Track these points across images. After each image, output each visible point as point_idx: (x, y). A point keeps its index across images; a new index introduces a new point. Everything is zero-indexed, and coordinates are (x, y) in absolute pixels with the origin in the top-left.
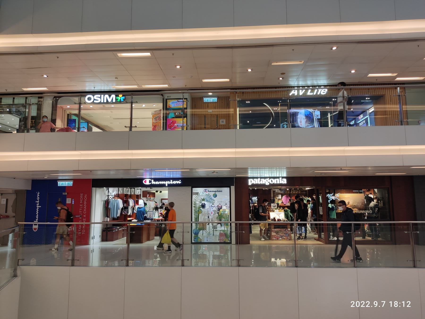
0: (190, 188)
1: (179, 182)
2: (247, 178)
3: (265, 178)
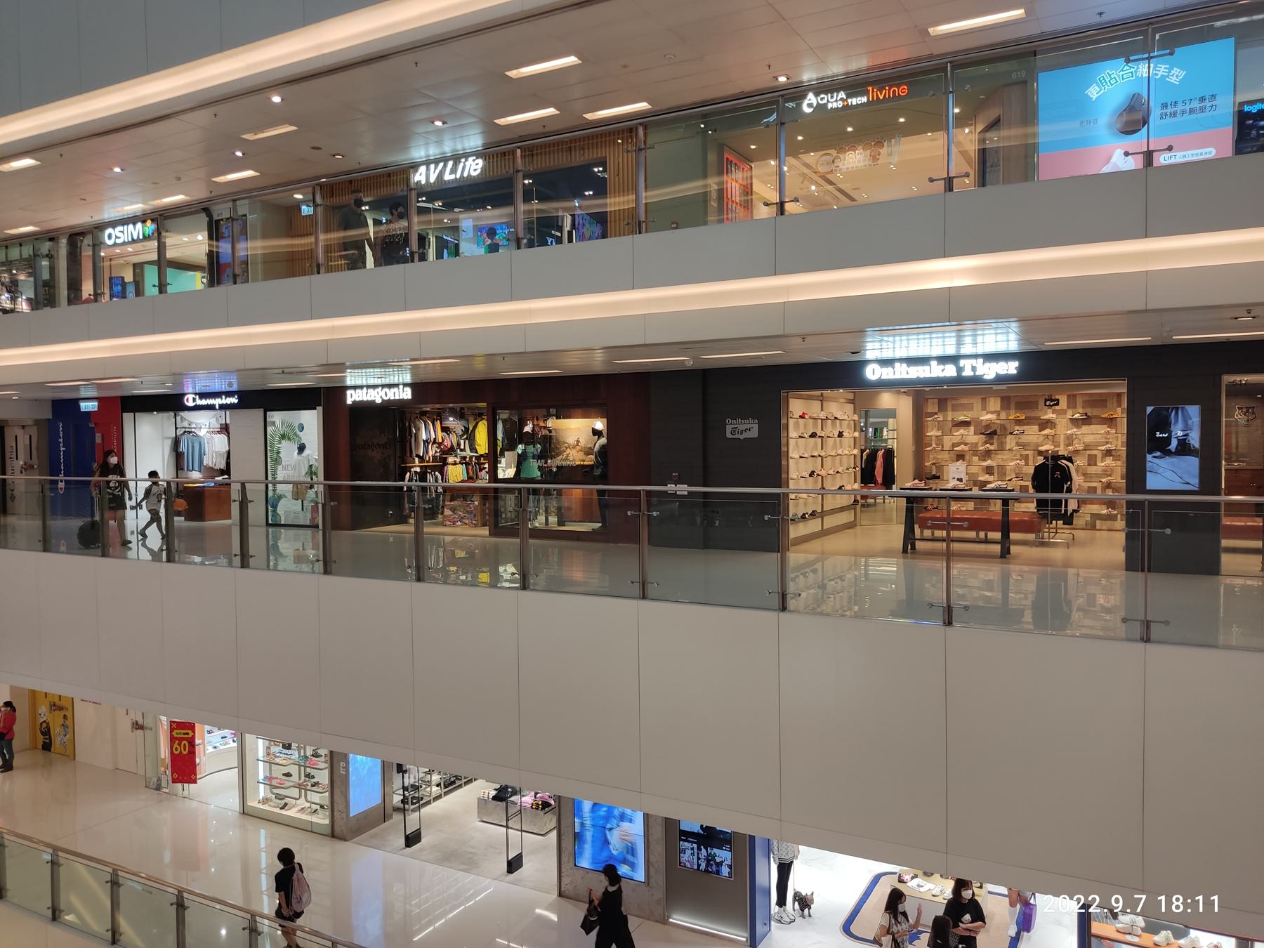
0: (260, 412)
1: (234, 400)
2: (865, 363)
3: (374, 387)
